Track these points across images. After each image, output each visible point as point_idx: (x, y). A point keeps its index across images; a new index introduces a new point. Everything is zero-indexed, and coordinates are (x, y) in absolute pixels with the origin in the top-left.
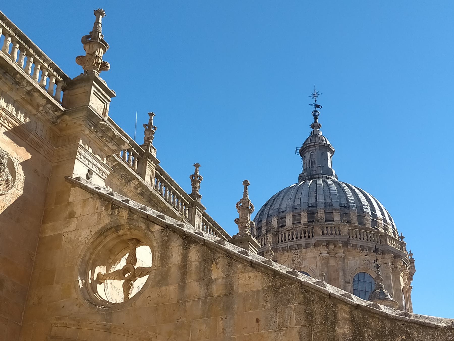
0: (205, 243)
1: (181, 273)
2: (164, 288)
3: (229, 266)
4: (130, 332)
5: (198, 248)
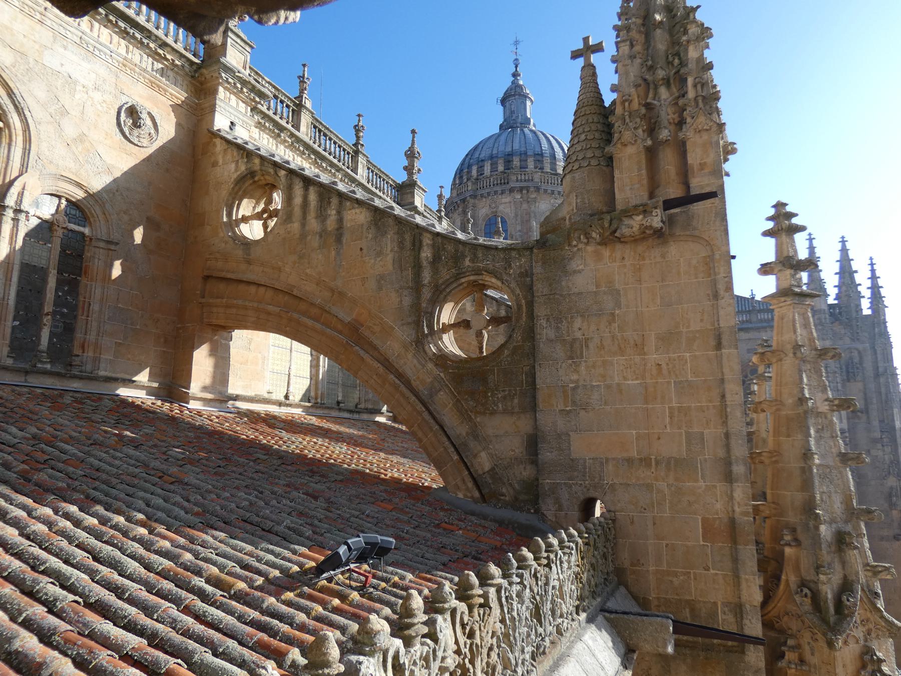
0: (321, 185)
2: (289, 226)
5: (316, 188)
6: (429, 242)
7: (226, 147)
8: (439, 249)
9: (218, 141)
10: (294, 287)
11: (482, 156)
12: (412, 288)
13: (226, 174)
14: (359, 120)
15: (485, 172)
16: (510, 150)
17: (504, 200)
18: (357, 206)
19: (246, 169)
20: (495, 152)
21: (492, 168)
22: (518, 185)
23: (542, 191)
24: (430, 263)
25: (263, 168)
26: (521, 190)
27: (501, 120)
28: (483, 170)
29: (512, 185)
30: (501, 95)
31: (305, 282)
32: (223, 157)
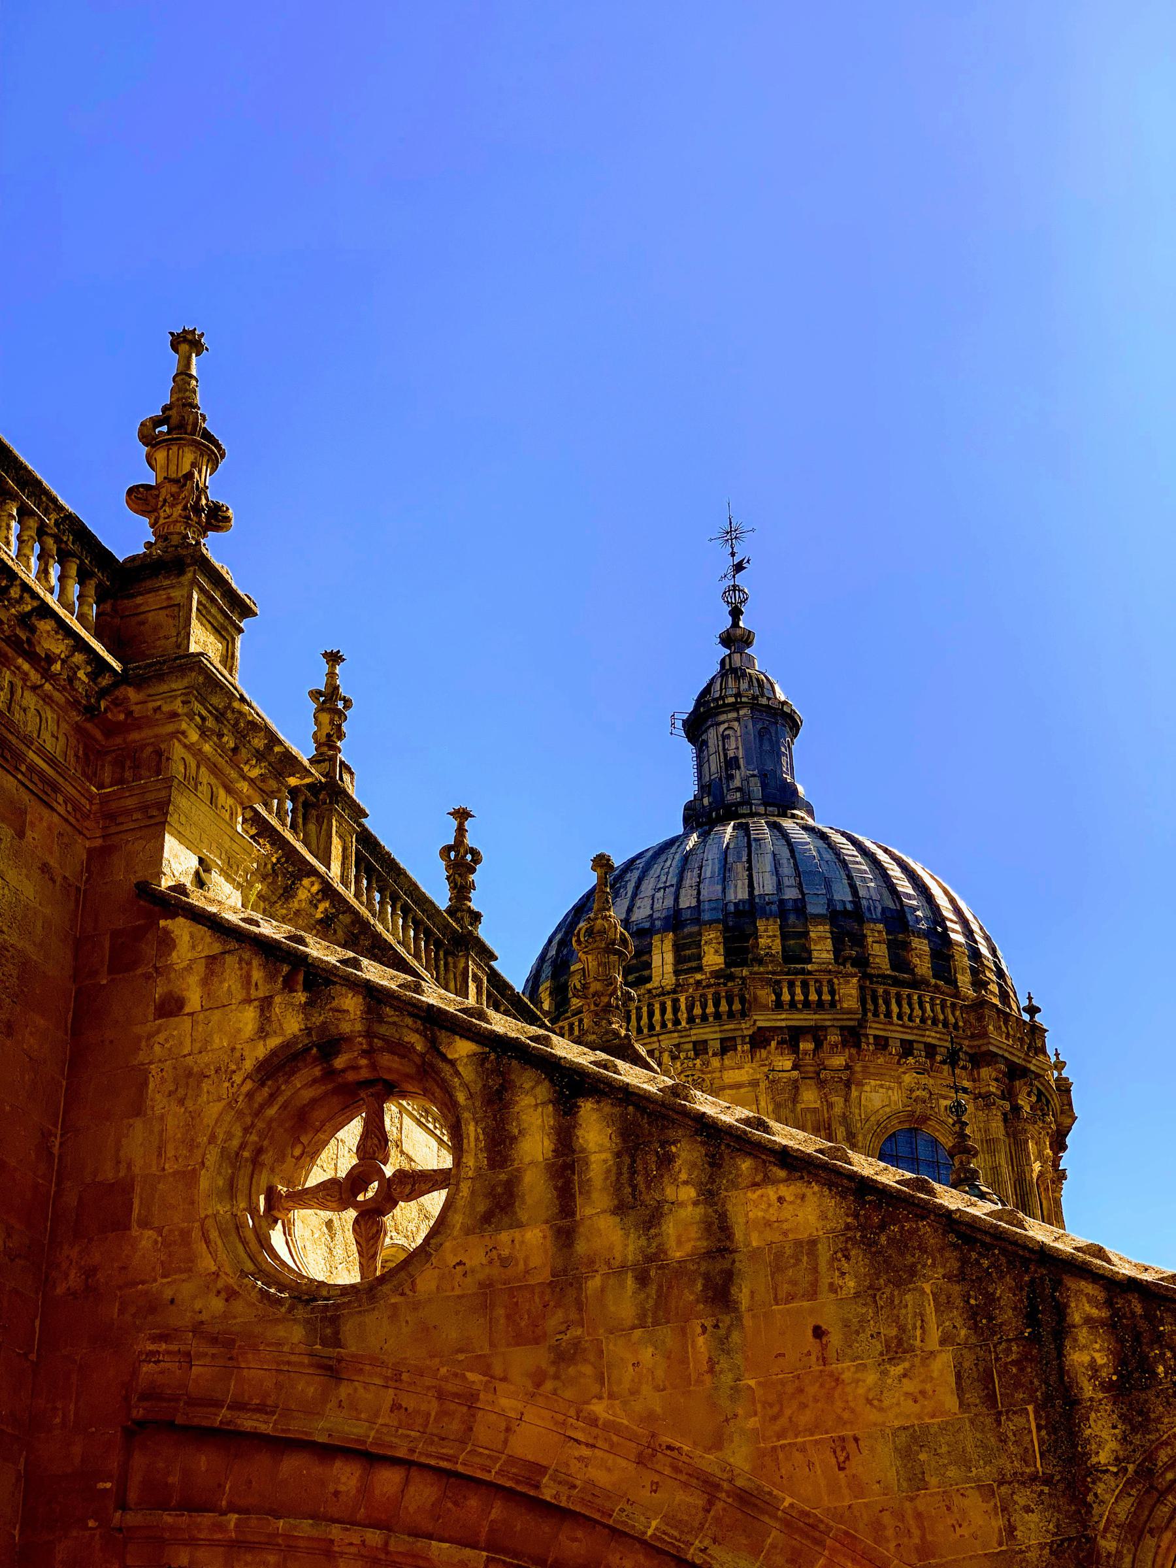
0: (627, 1095)
1: (556, 1188)
2: (504, 1237)
3: (711, 1165)
4: (405, 1376)
5: (608, 1109)
6: (1095, 1312)
7: (217, 948)
8: (1137, 1337)
9: (180, 928)
10: (542, 1470)
11: (641, 913)
12: (1048, 1480)
13: (220, 1042)
14: (461, 831)
15: (656, 973)
16: (742, 894)
18: (782, 1174)
19: (308, 1030)
20: (687, 901)
21: (679, 960)
22: (782, 1020)
23: (868, 1046)
24: (1107, 1387)
25: (383, 1030)
26: (792, 1038)
27: (690, 790)
28: (648, 965)
29: (763, 1020)
30: (688, 706)
31: (586, 1452)
32: (205, 982)
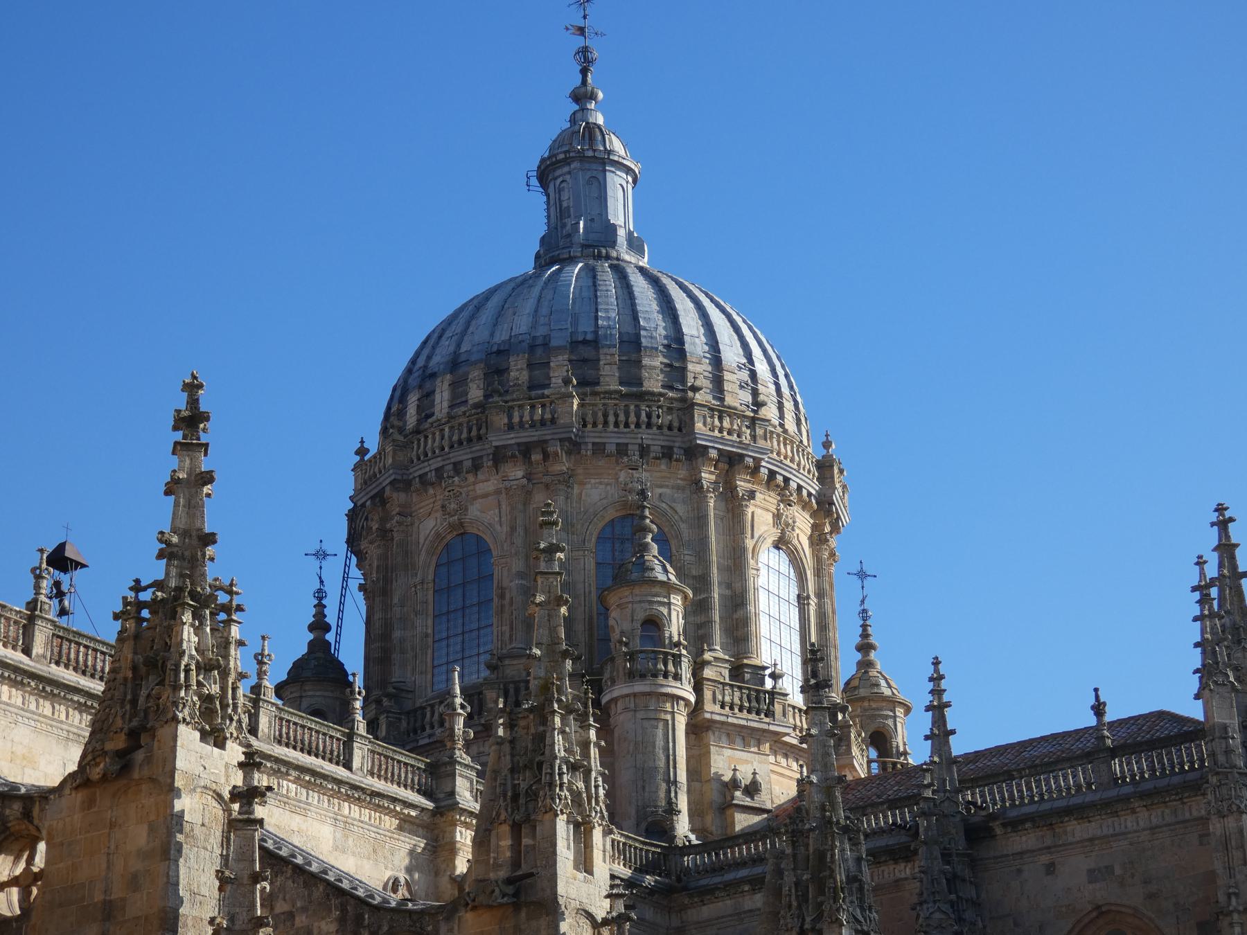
15: (437, 409)
17: (482, 488)
22: (511, 439)
23: (587, 451)
28: (433, 405)
